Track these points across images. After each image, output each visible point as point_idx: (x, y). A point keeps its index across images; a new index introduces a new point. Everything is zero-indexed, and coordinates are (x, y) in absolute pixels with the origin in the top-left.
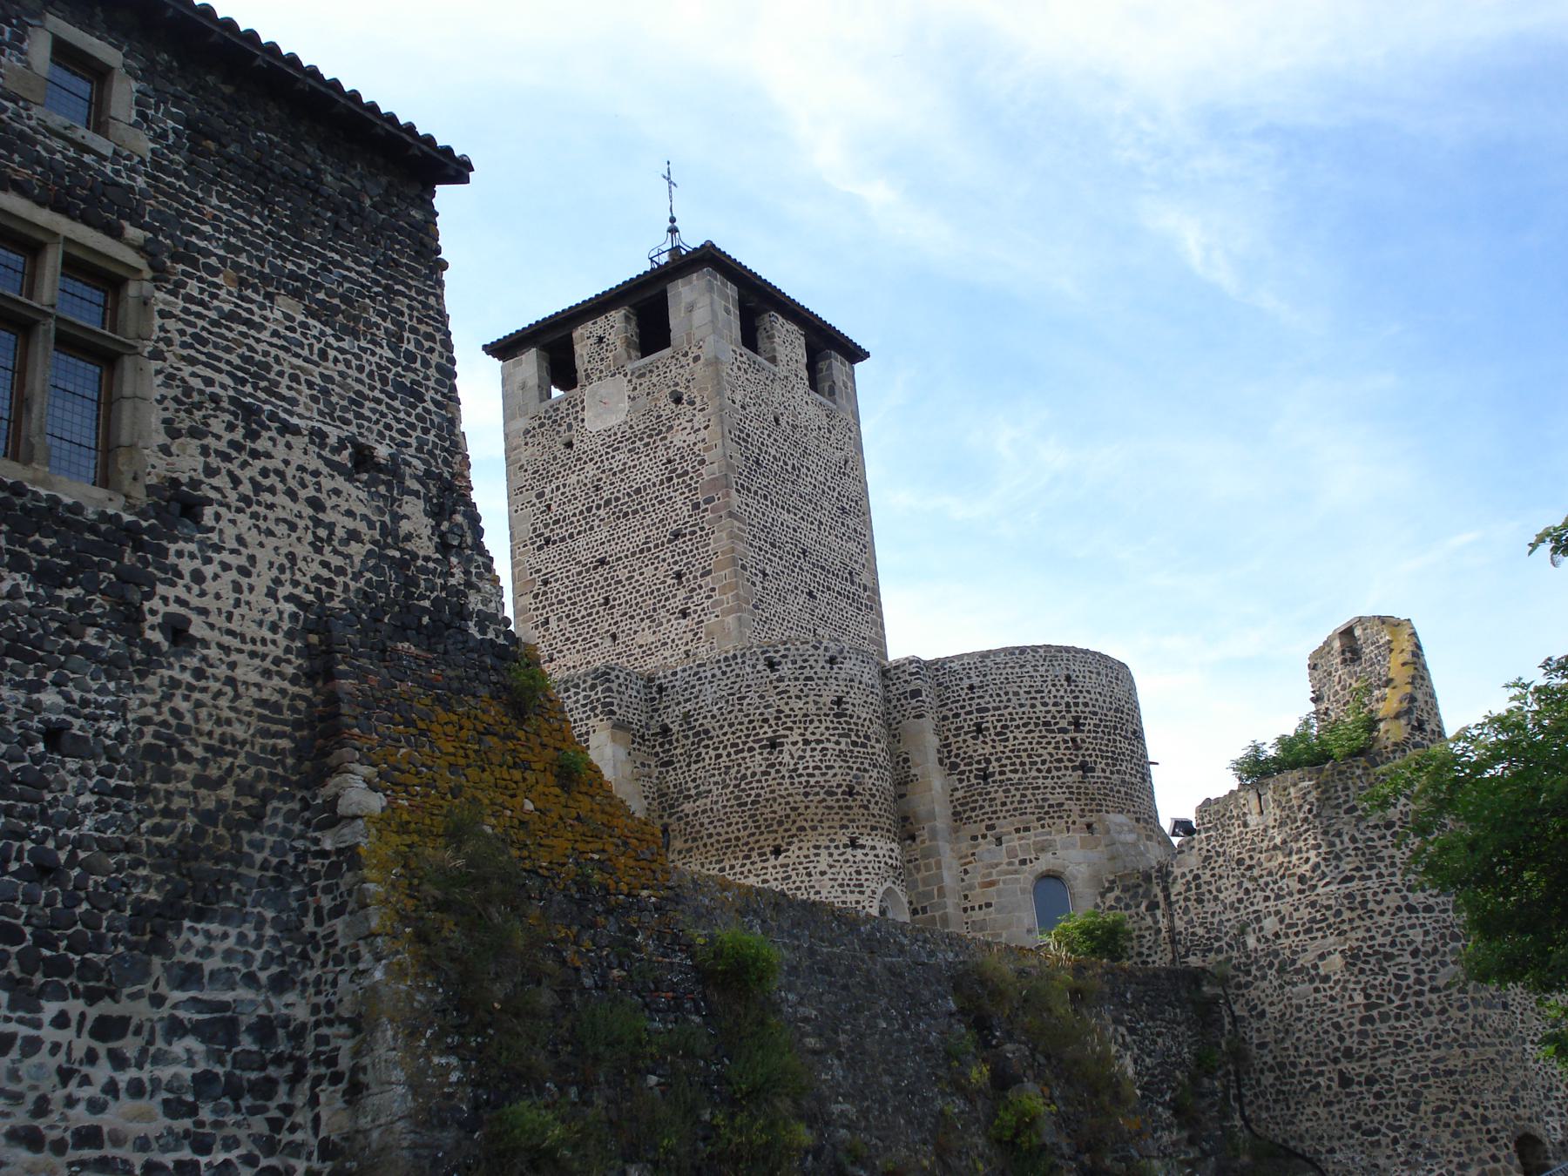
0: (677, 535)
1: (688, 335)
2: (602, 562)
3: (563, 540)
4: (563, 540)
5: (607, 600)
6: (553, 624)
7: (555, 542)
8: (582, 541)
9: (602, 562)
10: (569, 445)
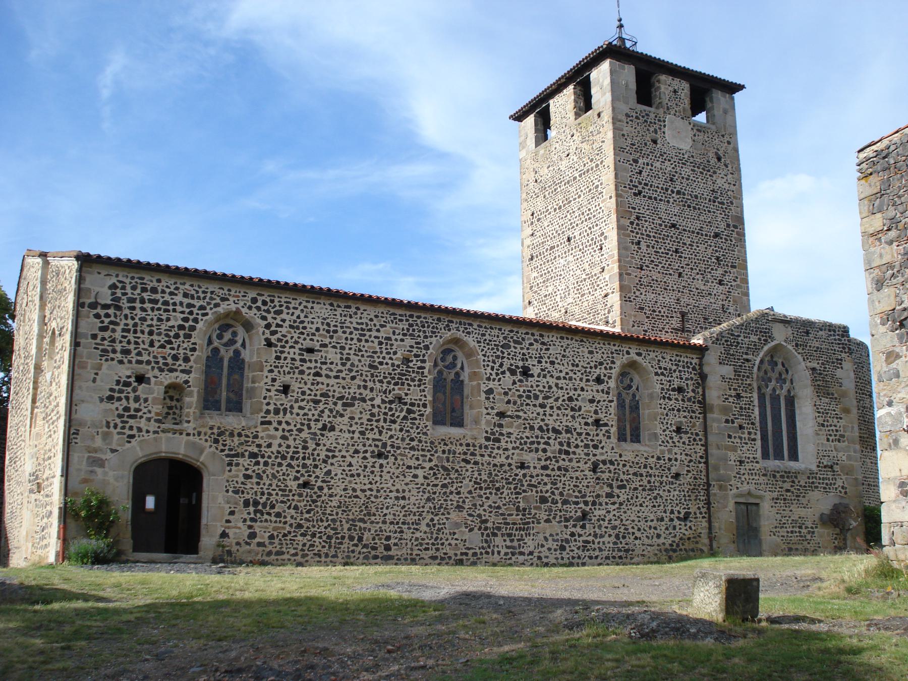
0: (716, 235)
1: (725, 126)
2: (674, 226)
3: (650, 198)
4: (650, 198)
5: (676, 251)
6: (643, 245)
7: (644, 196)
8: (662, 206)
9: (674, 226)
10: (655, 142)
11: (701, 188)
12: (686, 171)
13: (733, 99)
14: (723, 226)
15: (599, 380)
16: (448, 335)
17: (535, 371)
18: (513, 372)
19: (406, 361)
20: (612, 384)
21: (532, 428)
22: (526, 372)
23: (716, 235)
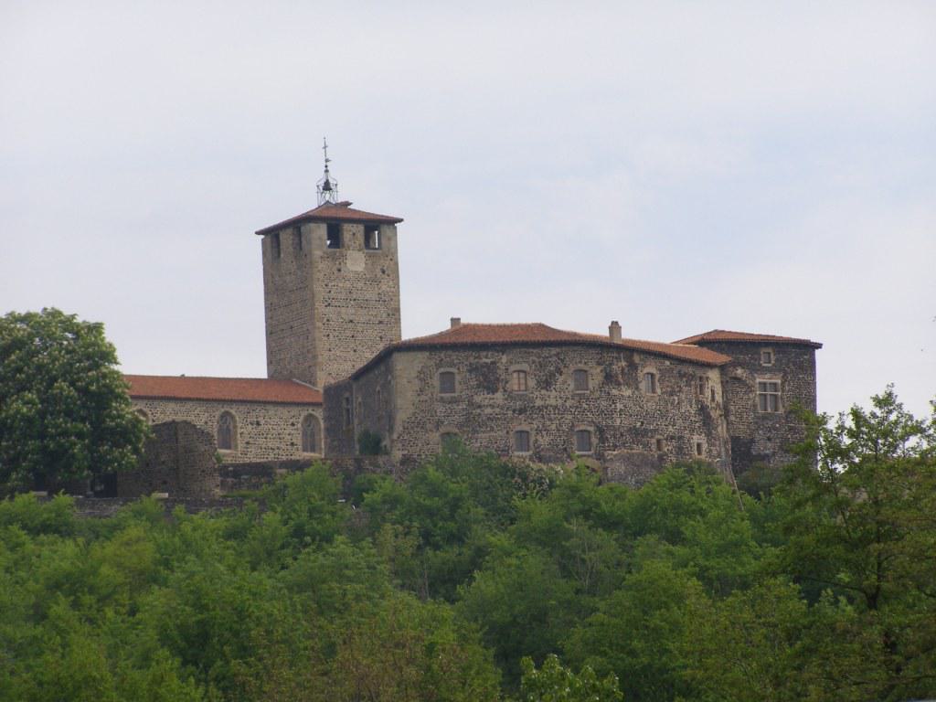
0: (381, 322)
2: (351, 321)
5: (353, 337)
6: (331, 336)
8: (343, 310)
9: (351, 321)
10: (339, 270)
11: (371, 294)
12: (360, 285)
13: (396, 228)
14: (384, 315)
15: (293, 424)
16: (223, 410)
17: (262, 422)
18: (252, 424)
19: (206, 423)
20: (299, 425)
21: (261, 448)
22: (258, 424)
23: (381, 322)
